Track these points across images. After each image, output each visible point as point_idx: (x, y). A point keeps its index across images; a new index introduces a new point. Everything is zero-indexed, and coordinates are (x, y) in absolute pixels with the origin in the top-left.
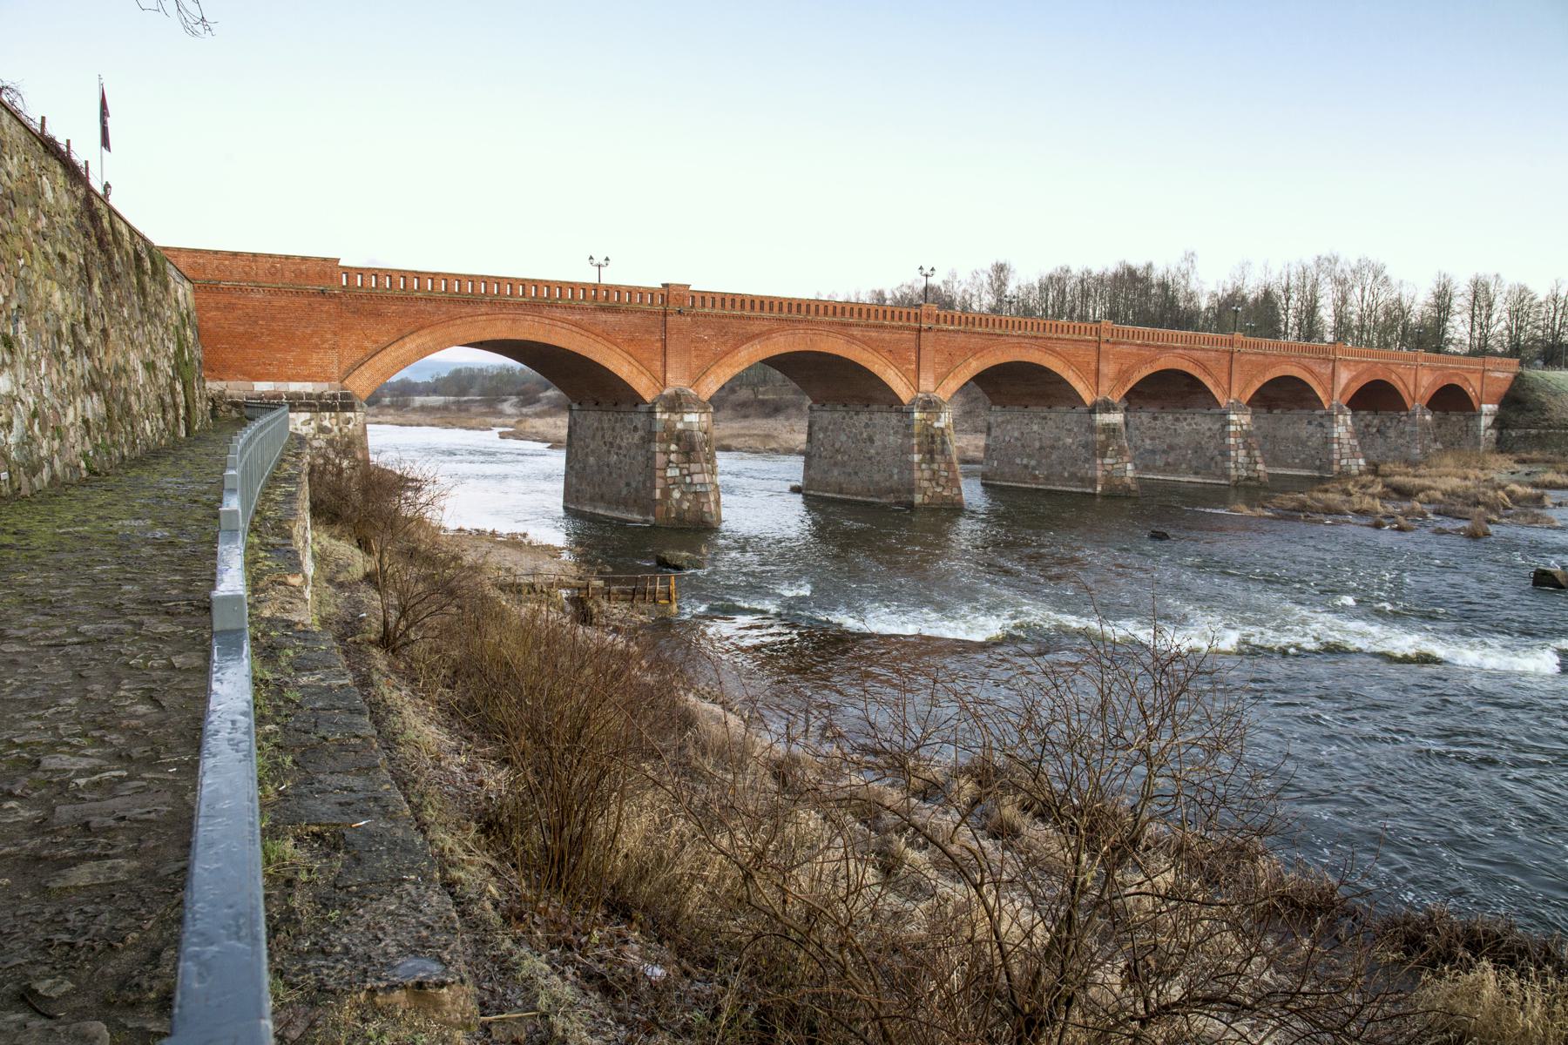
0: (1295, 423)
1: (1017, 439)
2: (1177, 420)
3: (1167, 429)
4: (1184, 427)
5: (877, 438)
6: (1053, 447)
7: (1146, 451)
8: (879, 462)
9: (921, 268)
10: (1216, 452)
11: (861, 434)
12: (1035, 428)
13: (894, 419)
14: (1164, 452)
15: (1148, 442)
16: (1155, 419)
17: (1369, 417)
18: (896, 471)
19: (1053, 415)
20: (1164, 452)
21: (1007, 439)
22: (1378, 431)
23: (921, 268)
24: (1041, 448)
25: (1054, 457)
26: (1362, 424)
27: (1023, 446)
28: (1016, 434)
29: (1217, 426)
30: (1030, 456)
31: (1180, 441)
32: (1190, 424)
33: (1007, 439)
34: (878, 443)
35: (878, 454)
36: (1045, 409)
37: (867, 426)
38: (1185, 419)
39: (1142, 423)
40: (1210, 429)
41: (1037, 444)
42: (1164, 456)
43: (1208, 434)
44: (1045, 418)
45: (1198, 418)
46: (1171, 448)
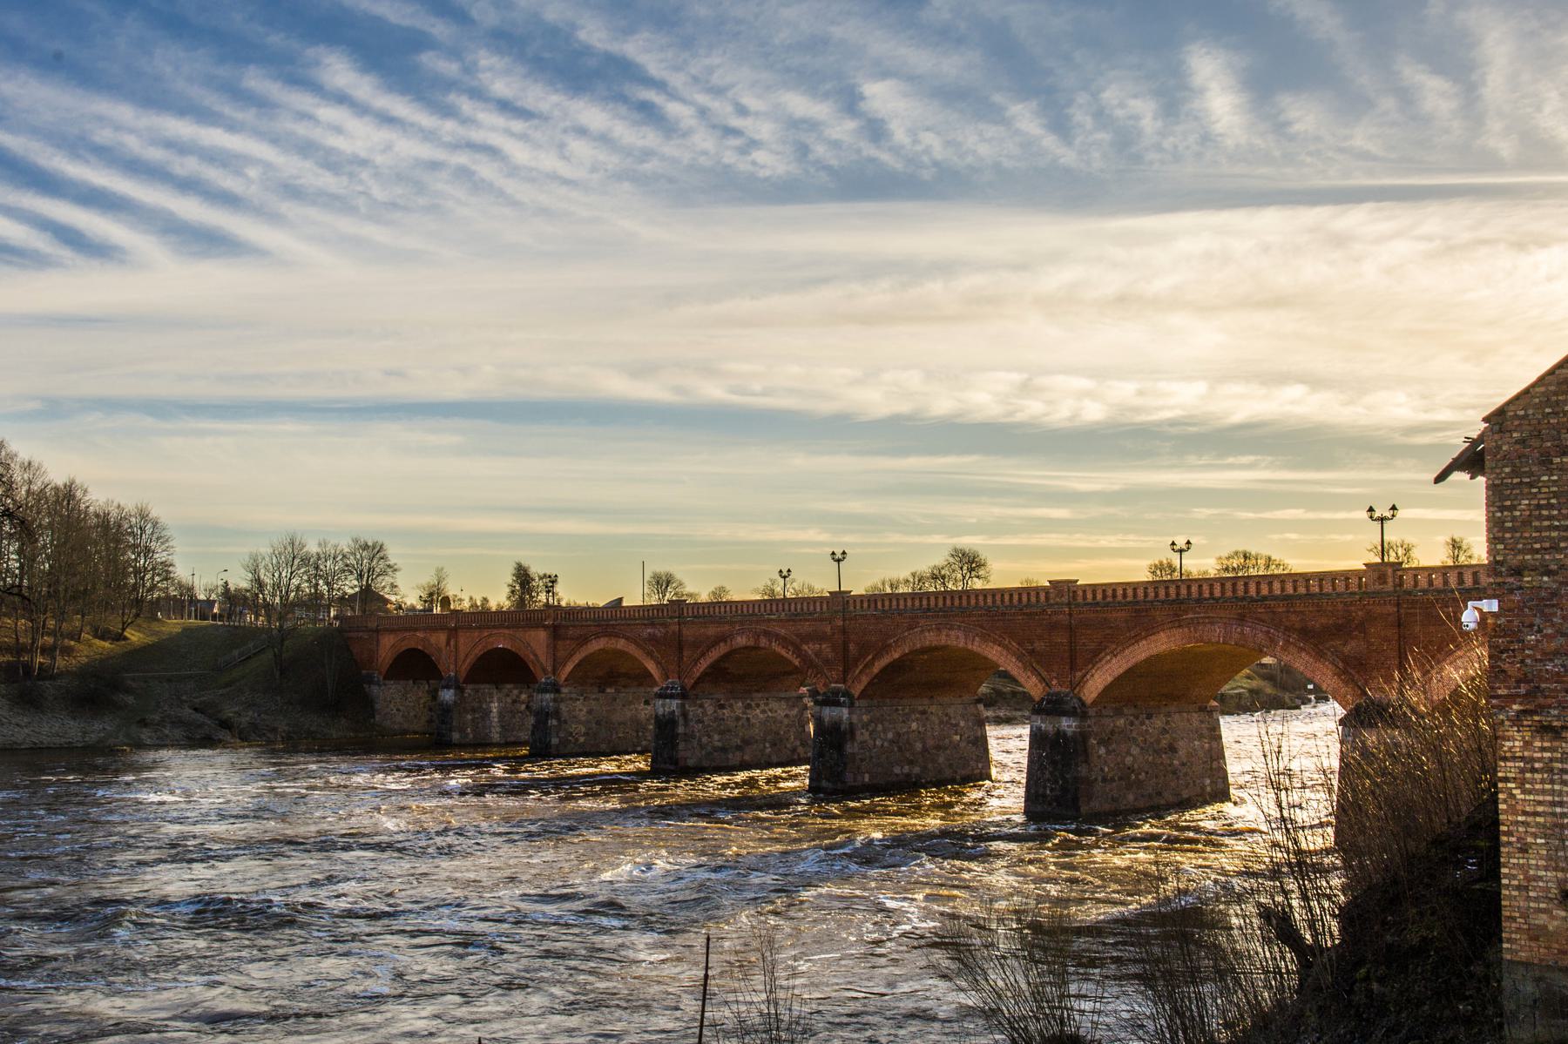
0: (631, 703)
1: (892, 742)
2: (749, 707)
3: (738, 719)
4: (757, 715)
5: (1181, 744)
6: (938, 748)
7: (715, 749)
8: (1186, 774)
9: (1173, 544)
10: (798, 743)
11: (1158, 741)
12: (914, 725)
13: (1195, 718)
14: (738, 748)
15: (716, 737)
16: (722, 707)
17: (516, 692)
18: (1208, 781)
19: (933, 709)
20: (738, 748)
21: (878, 743)
22: (527, 707)
23: (1173, 544)
24: (925, 749)
25: (941, 760)
26: (509, 700)
27: (900, 749)
28: (890, 735)
29: (795, 712)
30: (911, 763)
31: (756, 732)
32: (763, 712)
33: (878, 743)
34: (1182, 753)
35: (1183, 764)
36: (926, 701)
37: (1165, 731)
38: (758, 705)
39: (705, 713)
40: (787, 716)
41: (919, 746)
42: (738, 753)
43: (786, 721)
44: (924, 712)
45: (774, 705)
46: (747, 742)
